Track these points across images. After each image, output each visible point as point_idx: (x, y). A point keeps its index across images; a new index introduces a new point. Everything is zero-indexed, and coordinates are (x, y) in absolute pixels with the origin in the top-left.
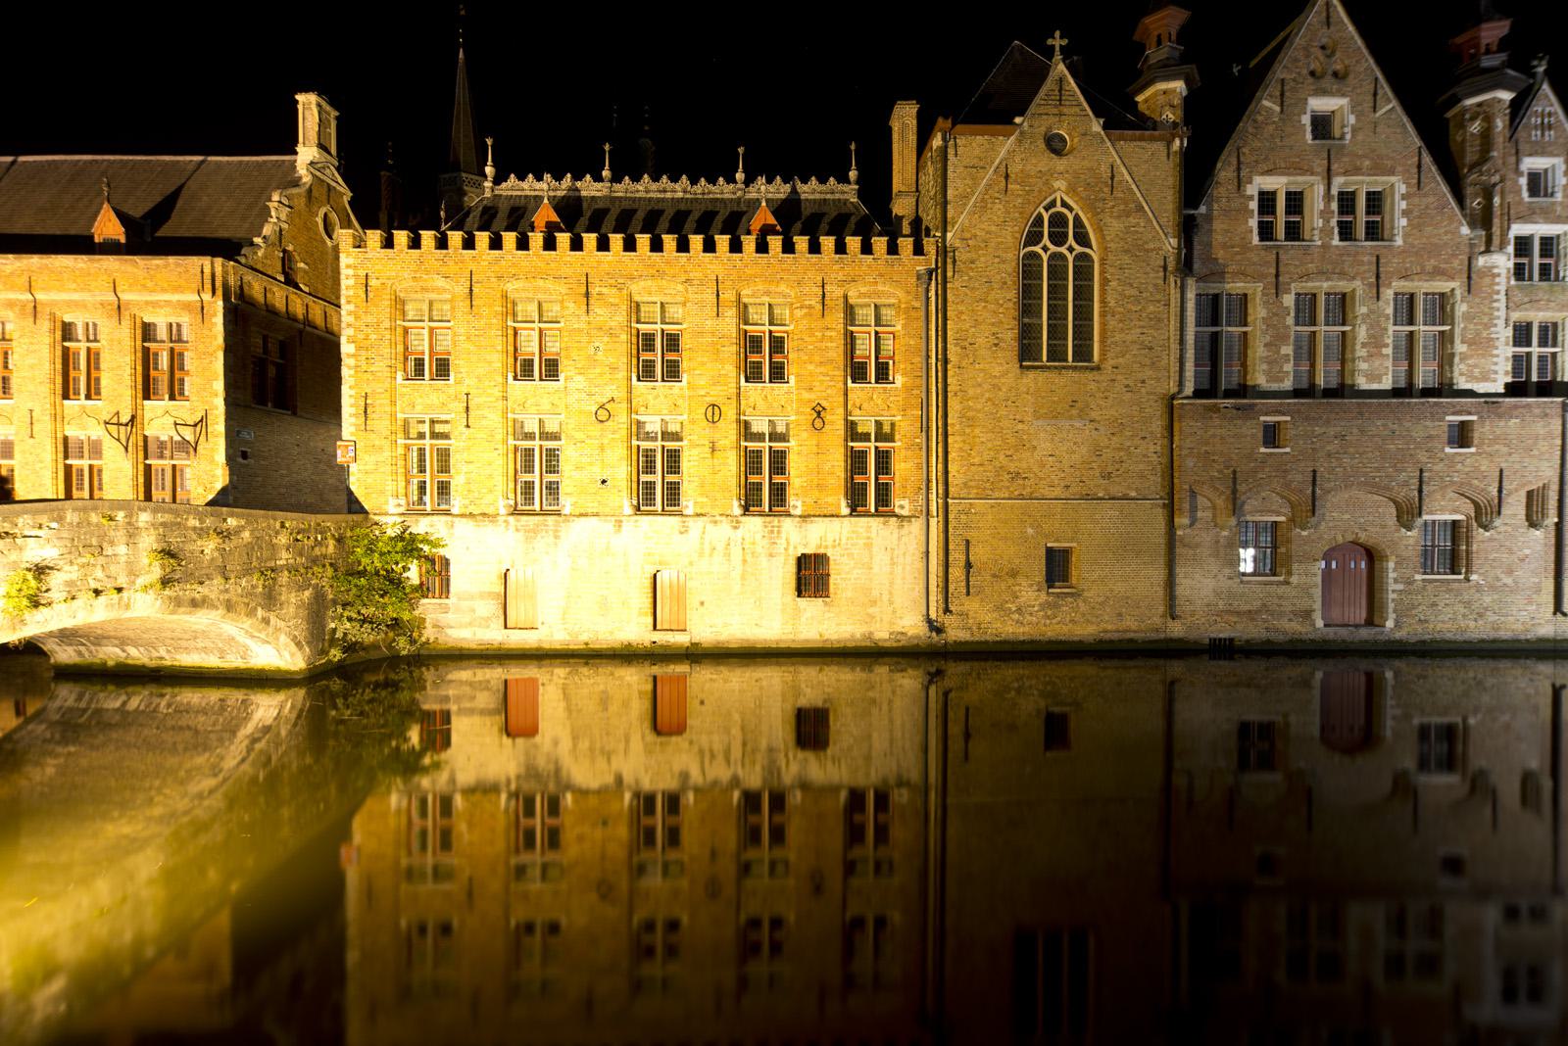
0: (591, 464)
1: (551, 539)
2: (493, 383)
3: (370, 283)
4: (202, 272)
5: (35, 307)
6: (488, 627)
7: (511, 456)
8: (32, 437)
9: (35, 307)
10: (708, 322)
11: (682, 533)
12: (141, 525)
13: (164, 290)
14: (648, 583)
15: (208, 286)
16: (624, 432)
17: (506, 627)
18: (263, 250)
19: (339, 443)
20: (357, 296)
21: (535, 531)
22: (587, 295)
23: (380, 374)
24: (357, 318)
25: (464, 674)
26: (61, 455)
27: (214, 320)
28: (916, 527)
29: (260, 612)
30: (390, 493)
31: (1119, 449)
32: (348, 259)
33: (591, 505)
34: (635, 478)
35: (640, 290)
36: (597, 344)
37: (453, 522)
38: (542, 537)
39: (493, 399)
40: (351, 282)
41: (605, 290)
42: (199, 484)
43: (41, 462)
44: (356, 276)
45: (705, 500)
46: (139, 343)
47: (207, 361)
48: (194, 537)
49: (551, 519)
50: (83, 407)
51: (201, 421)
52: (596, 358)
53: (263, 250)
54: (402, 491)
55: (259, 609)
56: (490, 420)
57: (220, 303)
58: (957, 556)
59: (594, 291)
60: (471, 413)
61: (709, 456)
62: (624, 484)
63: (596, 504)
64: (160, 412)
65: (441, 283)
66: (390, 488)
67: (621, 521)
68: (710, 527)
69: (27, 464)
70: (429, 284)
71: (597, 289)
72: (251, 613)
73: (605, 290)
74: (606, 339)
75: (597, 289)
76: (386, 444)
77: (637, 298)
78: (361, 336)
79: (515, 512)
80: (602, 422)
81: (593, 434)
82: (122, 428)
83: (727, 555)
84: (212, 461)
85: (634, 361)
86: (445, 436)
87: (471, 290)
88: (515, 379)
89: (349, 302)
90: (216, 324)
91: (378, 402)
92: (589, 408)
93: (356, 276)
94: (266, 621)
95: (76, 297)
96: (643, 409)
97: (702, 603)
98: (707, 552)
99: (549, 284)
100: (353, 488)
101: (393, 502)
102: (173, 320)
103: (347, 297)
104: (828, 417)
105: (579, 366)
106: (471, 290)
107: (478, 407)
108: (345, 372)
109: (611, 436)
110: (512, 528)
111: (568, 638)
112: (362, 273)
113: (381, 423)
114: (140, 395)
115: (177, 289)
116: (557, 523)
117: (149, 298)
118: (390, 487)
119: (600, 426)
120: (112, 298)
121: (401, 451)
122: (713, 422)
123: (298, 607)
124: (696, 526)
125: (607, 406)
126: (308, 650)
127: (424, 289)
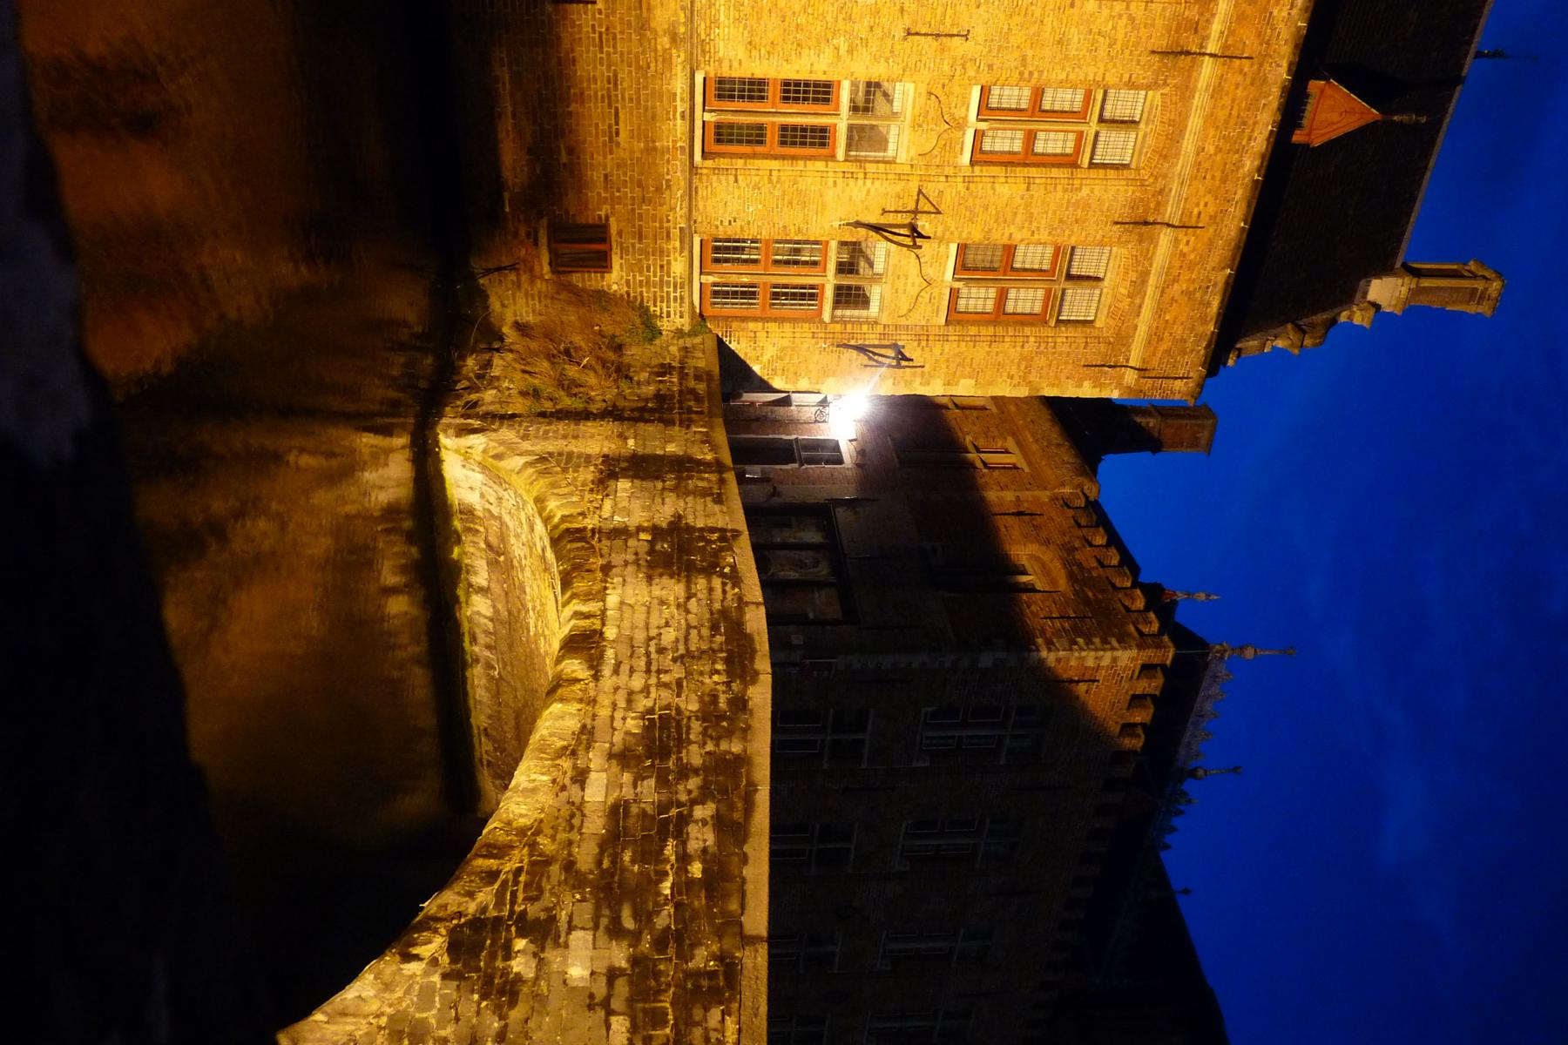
5: (1188, 53)
9: (1188, 53)
13: (1160, 311)
27: (1086, 384)
32: (1127, 658)
40: (1090, 663)
42: (783, 349)
43: (850, 51)
44: (1098, 667)
47: (1014, 370)
50: (961, 125)
64: (929, 271)
69: (849, 19)
90: (1080, 386)
95: (1188, 144)
103: (1068, 659)
112: (1101, 675)
115: (1155, 337)
117: (1152, 280)
120: (1171, 212)
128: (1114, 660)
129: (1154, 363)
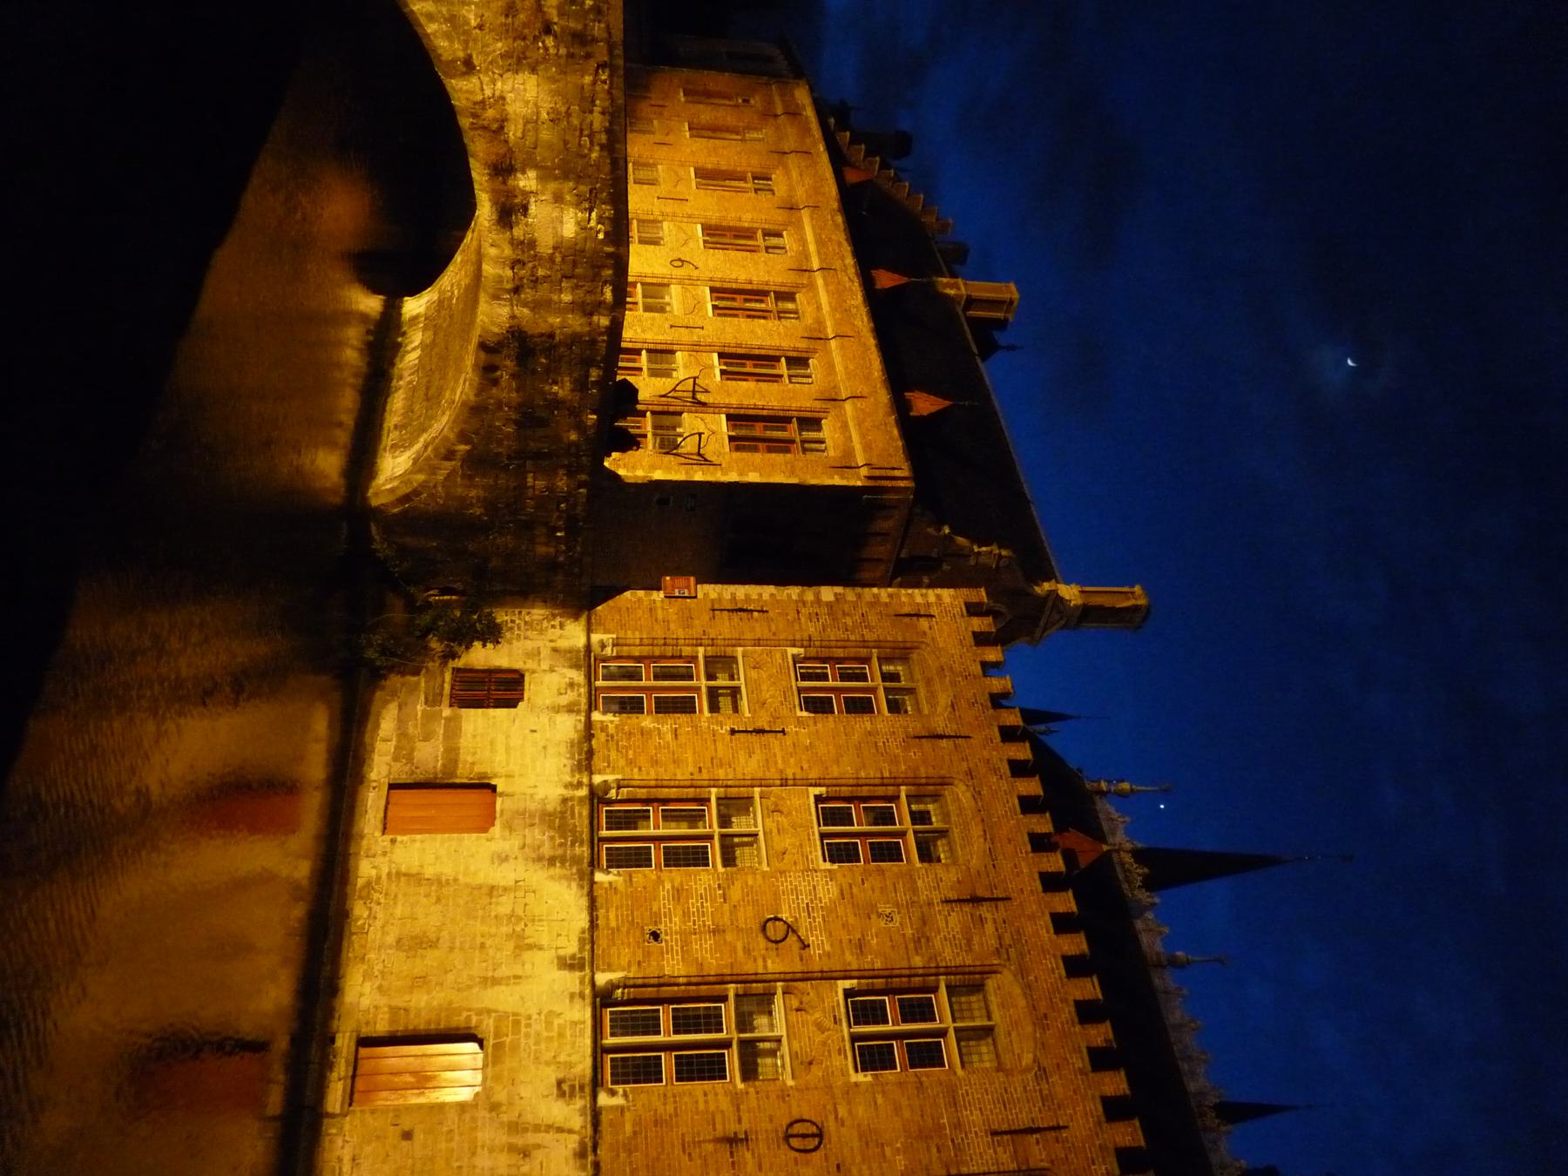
0: (686, 914)
1: (547, 850)
2: (806, 766)
3: (922, 619)
4: (894, 469)
5: (821, 339)
6: (396, 759)
7: (691, 792)
8: (672, 326)
10: (976, 1117)
11: (559, 1083)
12: (595, 318)
13: (863, 436)
14: (458, 1021)
15: (877, 473)
16: (749, 968)
17: (392, 787)
18: (934, 533)
19: (692, 579)
20: (902, 604)
21: (563, 829)
22: (976, 900)
23: (797, 627)
24: (872, 605)
25: (320, 724)
26: (651, 346)
29: (463, 448)
30: (622, 634)
33: (612, 915)
34: (667, 991)
35: (1003, 988)
36: (897, 918)
37: (578, 712)
38: (552, 838)
39: (780, 766)
40: (919, 599)
41: (989, 928)
45: (628, 1128)
46: (795, 414)
48: (575, 375)
49: (584, 851)
51: (706, 460)
52: (874, 917)
53: (934, 533)
54: (625, 651)
55: (468, 447)
56: (748, 763)
57: (859, 483)
59: (985, 911)
60: (754, 738)
61: (719, 1133)
62: (651, 970)
63: (613, 924)
65: (944, 700)
66: (630, 634)
67: (581, 968)
68: (573, 1142)
70: (937, 687)
71: (989, 916)
72: (463, 437)
73: (989, 928)
74: (909, 932)
75: (989, 916)
76: (696, 632)
77: (991, 984)
78: (846, 607)
79: (597, 797)
80: (764, 929)
81: (741, 914)
82: (690, 395)
84: (653, 467)
85: (879, 983)
86: (714, 707)
87: (941, 737)
88: (818, 799)
89: (890, 596)
91: (757, 625)
92: (785, 907)
93: (928, 605)
94: (449, 455)
96: (795, 1004)
97: (407, 1136)
98: (519, 1141)
99: (979, 844)
100: (628, 594)
101: (608, 638)
102: (829, 443)
105: (855, 890)
106: (941, 737)
107: (766, 746)
108: (794, 592)
109: (739, 945)
110: (568, 793)
111: (360, 882)
112: (934, 611)
113: (725, 627)
114: (732, 411)
115: (867, 447)
116: (576, 860)
117: (851, 424)
118: (632, 636)
119: (756, 927)
121: (687, 651)
122: (787, 1137)
123: (462, 499)
124: (571, 1114)
125: (792, 939)
126: (396, 510)
127: (929, 682)
128: (938, 597)
129: (875, 461)
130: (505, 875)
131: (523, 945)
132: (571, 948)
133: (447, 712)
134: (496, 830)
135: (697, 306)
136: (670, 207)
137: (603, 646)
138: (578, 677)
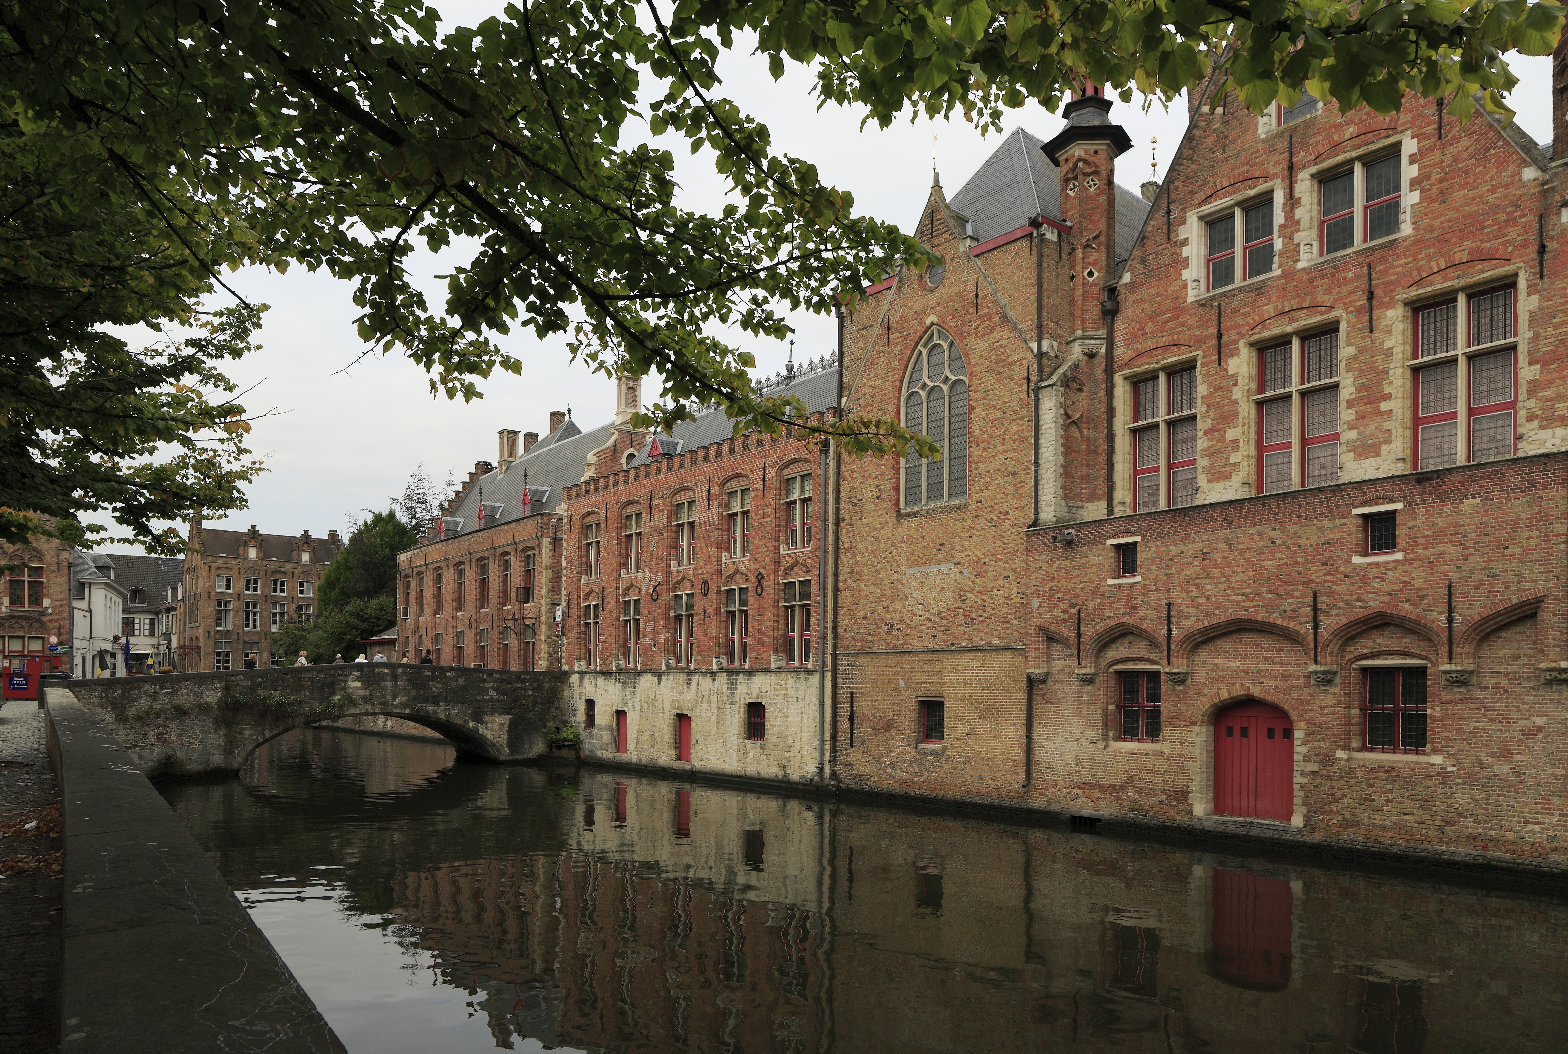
0: (650, 633)
1: (632, 689)
28: (815, 679)
31: (982, 593)
58: (844, 708)
59: (654, 503)
60: (606, 600)
73: (658, 501)
83: (709, 702)
104: (766, 584)
130: (637, 705)
131: (655, 699)
132: (656, 678)
133: (595, 731)
134: (626, 709)
135: (486, 614)
136: (450, 629)
137: (579, 666)
138: (587, 677)
